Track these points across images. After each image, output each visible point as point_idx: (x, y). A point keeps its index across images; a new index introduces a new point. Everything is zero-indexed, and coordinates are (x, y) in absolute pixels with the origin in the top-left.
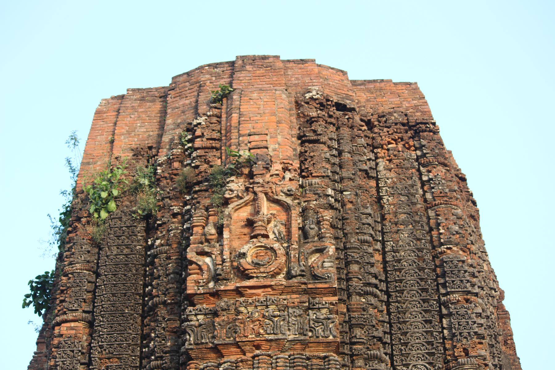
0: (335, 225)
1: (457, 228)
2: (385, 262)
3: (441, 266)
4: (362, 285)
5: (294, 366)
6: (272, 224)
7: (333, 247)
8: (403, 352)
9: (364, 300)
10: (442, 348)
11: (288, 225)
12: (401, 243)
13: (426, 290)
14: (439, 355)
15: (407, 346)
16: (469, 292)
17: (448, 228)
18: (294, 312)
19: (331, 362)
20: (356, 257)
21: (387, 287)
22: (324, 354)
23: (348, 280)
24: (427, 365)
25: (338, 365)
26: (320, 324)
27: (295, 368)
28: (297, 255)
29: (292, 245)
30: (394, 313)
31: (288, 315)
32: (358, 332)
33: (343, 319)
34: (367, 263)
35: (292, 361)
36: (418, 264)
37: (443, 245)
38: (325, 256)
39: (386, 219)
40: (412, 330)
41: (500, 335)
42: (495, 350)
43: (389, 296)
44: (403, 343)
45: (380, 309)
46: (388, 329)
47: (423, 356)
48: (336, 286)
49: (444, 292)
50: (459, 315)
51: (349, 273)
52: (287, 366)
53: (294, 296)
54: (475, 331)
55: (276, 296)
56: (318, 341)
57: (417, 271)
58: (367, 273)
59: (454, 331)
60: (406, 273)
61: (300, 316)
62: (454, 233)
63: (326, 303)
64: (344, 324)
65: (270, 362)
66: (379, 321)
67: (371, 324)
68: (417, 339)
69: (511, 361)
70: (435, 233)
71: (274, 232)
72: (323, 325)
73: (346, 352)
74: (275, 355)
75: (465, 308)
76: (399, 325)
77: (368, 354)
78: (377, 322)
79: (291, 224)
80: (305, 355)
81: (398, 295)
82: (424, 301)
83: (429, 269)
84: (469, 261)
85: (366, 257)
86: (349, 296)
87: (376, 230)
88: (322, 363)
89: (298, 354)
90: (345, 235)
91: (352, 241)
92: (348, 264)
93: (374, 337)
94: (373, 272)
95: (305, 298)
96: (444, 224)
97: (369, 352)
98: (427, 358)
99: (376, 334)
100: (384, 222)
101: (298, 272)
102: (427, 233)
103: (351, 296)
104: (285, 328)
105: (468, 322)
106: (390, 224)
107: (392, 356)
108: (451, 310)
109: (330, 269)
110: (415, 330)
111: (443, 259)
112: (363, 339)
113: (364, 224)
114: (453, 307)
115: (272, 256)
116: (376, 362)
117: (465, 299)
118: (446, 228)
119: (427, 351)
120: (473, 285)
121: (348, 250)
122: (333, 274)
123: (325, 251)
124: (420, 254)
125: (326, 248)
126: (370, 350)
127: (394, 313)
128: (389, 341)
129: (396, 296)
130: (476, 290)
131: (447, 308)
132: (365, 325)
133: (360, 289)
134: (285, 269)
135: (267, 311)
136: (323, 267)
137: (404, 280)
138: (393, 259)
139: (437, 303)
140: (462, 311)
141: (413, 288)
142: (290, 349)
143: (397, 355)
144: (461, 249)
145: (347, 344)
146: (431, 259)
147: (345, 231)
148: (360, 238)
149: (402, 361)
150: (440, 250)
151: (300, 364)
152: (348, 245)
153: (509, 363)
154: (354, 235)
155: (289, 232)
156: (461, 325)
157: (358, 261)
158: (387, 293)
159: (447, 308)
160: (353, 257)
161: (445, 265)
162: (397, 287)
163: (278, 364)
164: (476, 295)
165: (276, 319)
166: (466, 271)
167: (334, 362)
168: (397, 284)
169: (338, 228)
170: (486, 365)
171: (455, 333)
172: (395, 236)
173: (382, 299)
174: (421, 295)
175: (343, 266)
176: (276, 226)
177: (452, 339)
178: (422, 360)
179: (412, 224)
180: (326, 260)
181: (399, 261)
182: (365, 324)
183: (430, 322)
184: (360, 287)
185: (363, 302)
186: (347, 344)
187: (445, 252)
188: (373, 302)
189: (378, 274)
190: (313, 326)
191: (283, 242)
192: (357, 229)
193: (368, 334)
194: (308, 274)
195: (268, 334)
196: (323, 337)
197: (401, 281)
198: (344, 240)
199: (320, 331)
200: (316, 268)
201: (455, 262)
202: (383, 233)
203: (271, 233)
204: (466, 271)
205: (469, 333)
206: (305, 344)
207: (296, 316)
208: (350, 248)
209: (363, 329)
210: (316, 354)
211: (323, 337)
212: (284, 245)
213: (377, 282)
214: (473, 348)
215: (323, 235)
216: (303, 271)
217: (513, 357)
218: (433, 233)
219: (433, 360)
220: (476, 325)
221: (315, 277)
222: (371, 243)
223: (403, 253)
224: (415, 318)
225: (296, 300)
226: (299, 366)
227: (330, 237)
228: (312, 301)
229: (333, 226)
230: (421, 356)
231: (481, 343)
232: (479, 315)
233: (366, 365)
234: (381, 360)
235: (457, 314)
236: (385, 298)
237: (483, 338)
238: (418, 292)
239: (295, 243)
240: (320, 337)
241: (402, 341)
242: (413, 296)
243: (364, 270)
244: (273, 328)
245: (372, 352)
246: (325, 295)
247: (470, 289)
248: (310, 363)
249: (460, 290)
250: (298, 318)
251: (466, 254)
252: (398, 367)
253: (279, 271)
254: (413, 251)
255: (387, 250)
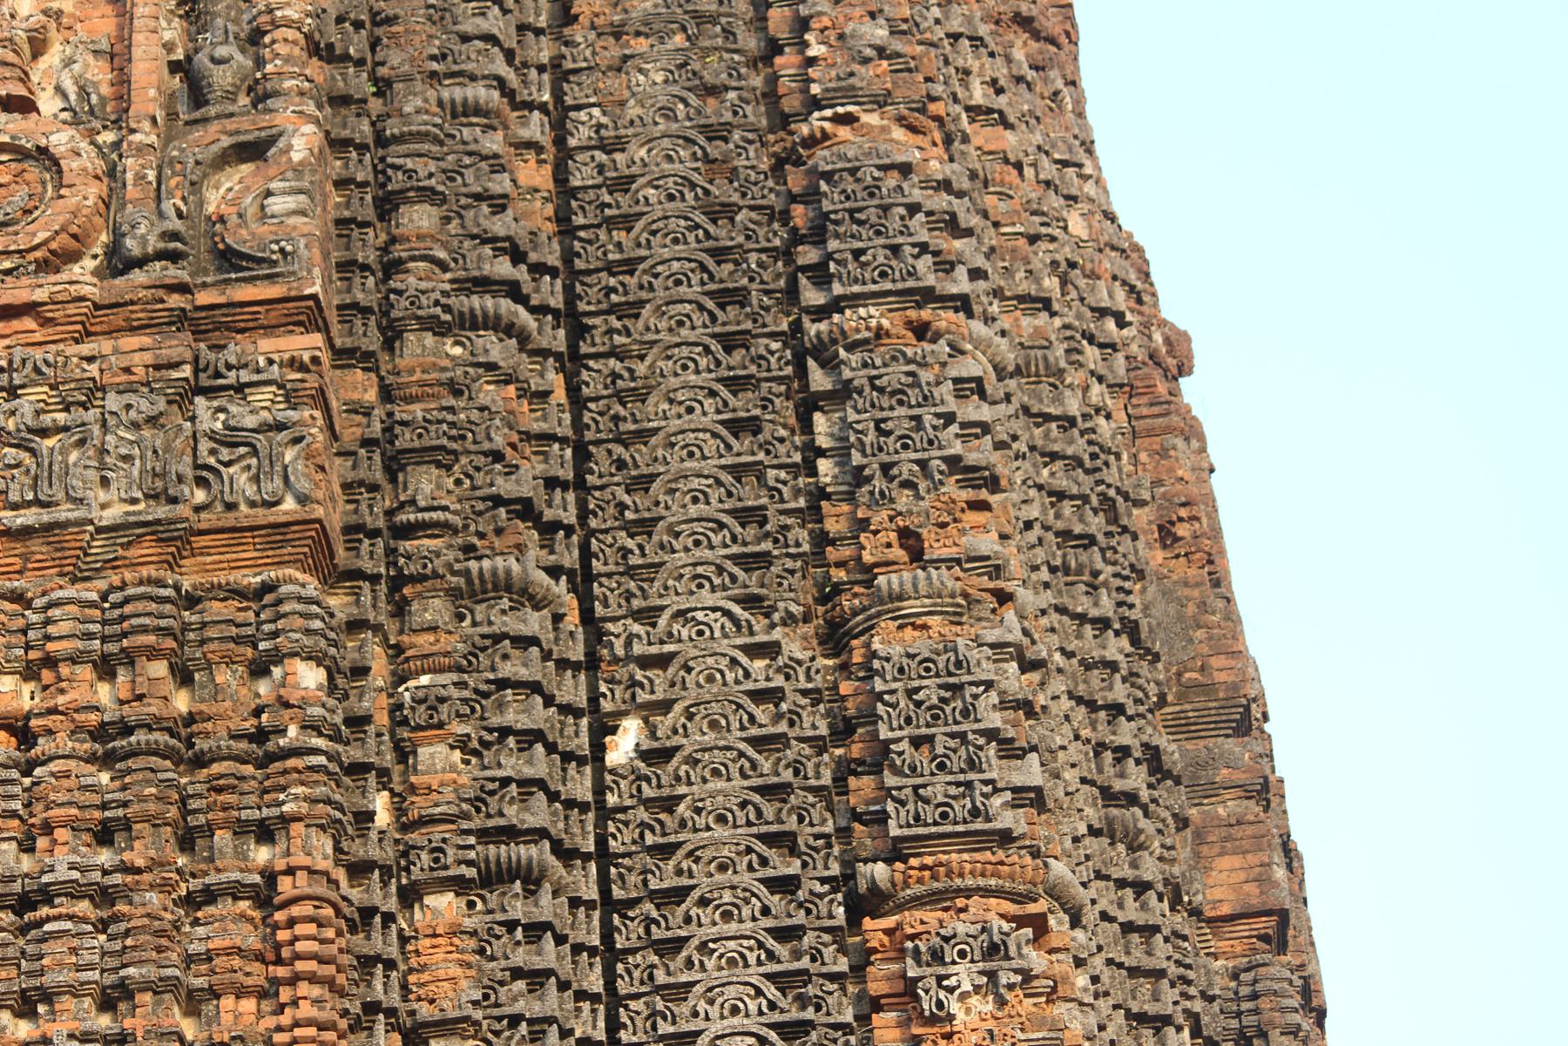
0: (330, 46)
1: (880, 33)
2: (564, 190)
3: (811, 196)
4: (447, 287)
5: (125, 635)
6: (53, 57)
7: (310, 128)
8: (635, 560)
9: (458, 351)
10: (803, 535)
11: (118, 56)
12: (633, 111)
13: (737, 297)
14: (789, 564)
15: (650, 534)
16: (927, 296)
17: (841, 37)
18: (129, 407)
19: (286, 608)
20: (422, 173)
21: (571, 297)
22: (258, 579)
23: (392, 267)
24: (736, 609)
25: (317, 616)
26: (242, 450)
27: (125, 643)
28: (151, 175)
29: (133, 131)
30: (597, 399)
31: (104, 424)
32: (425, 483)
33: (358, 431)
34: (478, 197)
35: (117, 612)
36: (707, 192)
37: (821, 108)
38: (272, 171)
39: (576, 18)
40: (675, 466)
41: (1141, 504)
42: (1097, 556)
43: (578, 331)
44: (634, 521)
45: (535, 384)
46: (569, 466)
47: (720, 570)
48: (316, 289)
49: (822, 301)
50: (881, 390)
51: (393, 240)
52: (89, 636)
53: (131, 342)
54: (952, 451)
55: (53, 347)
56: (231, 523)
57: (699, 218)
58: (473, 237)
59: (857, 458)
60: (654, 233)
61: (152, 421)
62: (869, 52)
63: (271, 362)
64: (363, 451)
65: (21, 623)
66: (527, 436)
67: (486, 446)
68: (695, 500)
69: (1191, 609)
70: (787, 62)
71: (60, 91)
72: (255, 452)
73: (367, 566)
74: (44, 594)
75: (909, 362)
76: (618, 450)
77: (467, 573)
78: (515, 438)
79: (130, 46)
80: (177, 588)
81: (617, 324)
82: (730, 342)
83: (752, 208)
84: (934, 164)
85: (469, 175)
86: (392, 337)
87: (525, 65)
88: (251, 614)
89: (141, 583)
90: (383, 87)
91: (408, 109)
92: (387, 205)
93: (498, 501)
94: (502, 233)
95: (178, 346)
96: (826, 22)
97: (473, 565)
98: (733, 578)
99: (505, 487)
100: (566, 31)
101: (154, 244)
102: (753, 63)
103: (399, 335)
104: (83, 477)
105: (918, 418)
106: (592, 36)
107: (582, 581)
108: (847, 374)
109: (292, 221)
110: (688, 464)
111: (816, 166)
112: (445, 509)
113: (465, 38)
114: (855, 359)
115: (44, 183)
116: (505, 603)
117: (909, 324)
118: (832, 36)
119: (735, 549)
120: (946, 266)
121: (393, 148)
122: (302, 242)
123: (273, 150)
124: (715, 150)
125: (281, 135)
126: (479, 558)
127: (597, 399)
128: (570, 517)
129: (610, 332)
130: (960, 283)
131: (830, 364)
132: (454, 452)
133: (437, 303)
134: (104, 238)
135: (13, 413)
136: (263, 214)
137: (644, 259)
138: (600, 180)
139: (785, 345)
140: (895, 375)
141: (683, 289)
142: (112, 564)
143: (609, 575)
144: (900, 119)
145: (374, 534)
146: (765, 164)
147: (383, 71)
148: (446, 95)
149: (629, 596)
150: (805, 130)
151: (146, 621)
152: (392, 128)
153: (1181, 618)
154: (419, 86)
155: (122, 80)
156: (888, 433)
157: (432, 189)
158: (573, 320)
159: (830, 364)
160: (410, 173)
161: (824, 186)
162: (614, 290)
163: (51, 629)
164: (963, 304)
165: (50, 442)
166: (913, 209)
167: (299, 607)
168: (612, 281)
169: (346, 57)
170: (1004, 598)
171: (862, 468)
172: (613, 83)
173: (545, 344)
174: (713, 318)
175: (369, 213)
176: (68, 63)
177: (850, 497)
178: (713, 589)
179: (684, 29)
180: (274, 185)
181: (623, 184)
182: (454, 446)
183: (751, 426)
184: (437, 295)
185: (453, 358)
186: (374, 534)
187: (826, 136)
188: (495, 355)
189: (524, 244)
190: (212, 461)
191: (97, 124)
192: (433, 58)
193: (474, 488)
194: (199, 250)
195: (15, 507)
196: (252, 504)
197: (630, 266)
198: (375, 105)
199: (243, 480)
200: (234, 219)
201: (869, 174)
202: (560, 74)
203: (50, 90)
204: (913, 209)
205: (923, 464)
206: (177, 540)
207: (136, 426)
208: (399, 139)
209: (449, 468)
210: (222, 578)
211: (252, 504)
212: (100, 139)
213: (521, 274)
214: (943, 525)
215: (268, 86)
216: (174, 236)
217: (1196, 593)
218: (778, 60)
219: (762, 586)
220: (954, 428)
221: (230, 260)
222: (498, 114)
223: (643, 152)
224: (684, 410)
225: (137, 358)
226: (144, 630)
227: (302, 94)
228: (212, 356)
229: (317, 49)
230: (709, 571)
231: (982, 506)
232: (974, 388)
233: (461, 618)
234: (526, 596)
235: (874, 387)
236: (558, 339)
237: (994, 484)
238: (701, 308)
239: (146, 125)
240: (243, 508)
241: (629, 515)
242: (680, 324)
243: (463, 226)
244: (36, 478)
245: (486, 563)
246: (270, 329)
247: (930, 280)
248: (194, 618)
249: (888, 286)
250: (147, 433)
251: (920, 140)
252: (610, 626)
253: (74, 244)
254: (687, 139)
255: (572, 142)
